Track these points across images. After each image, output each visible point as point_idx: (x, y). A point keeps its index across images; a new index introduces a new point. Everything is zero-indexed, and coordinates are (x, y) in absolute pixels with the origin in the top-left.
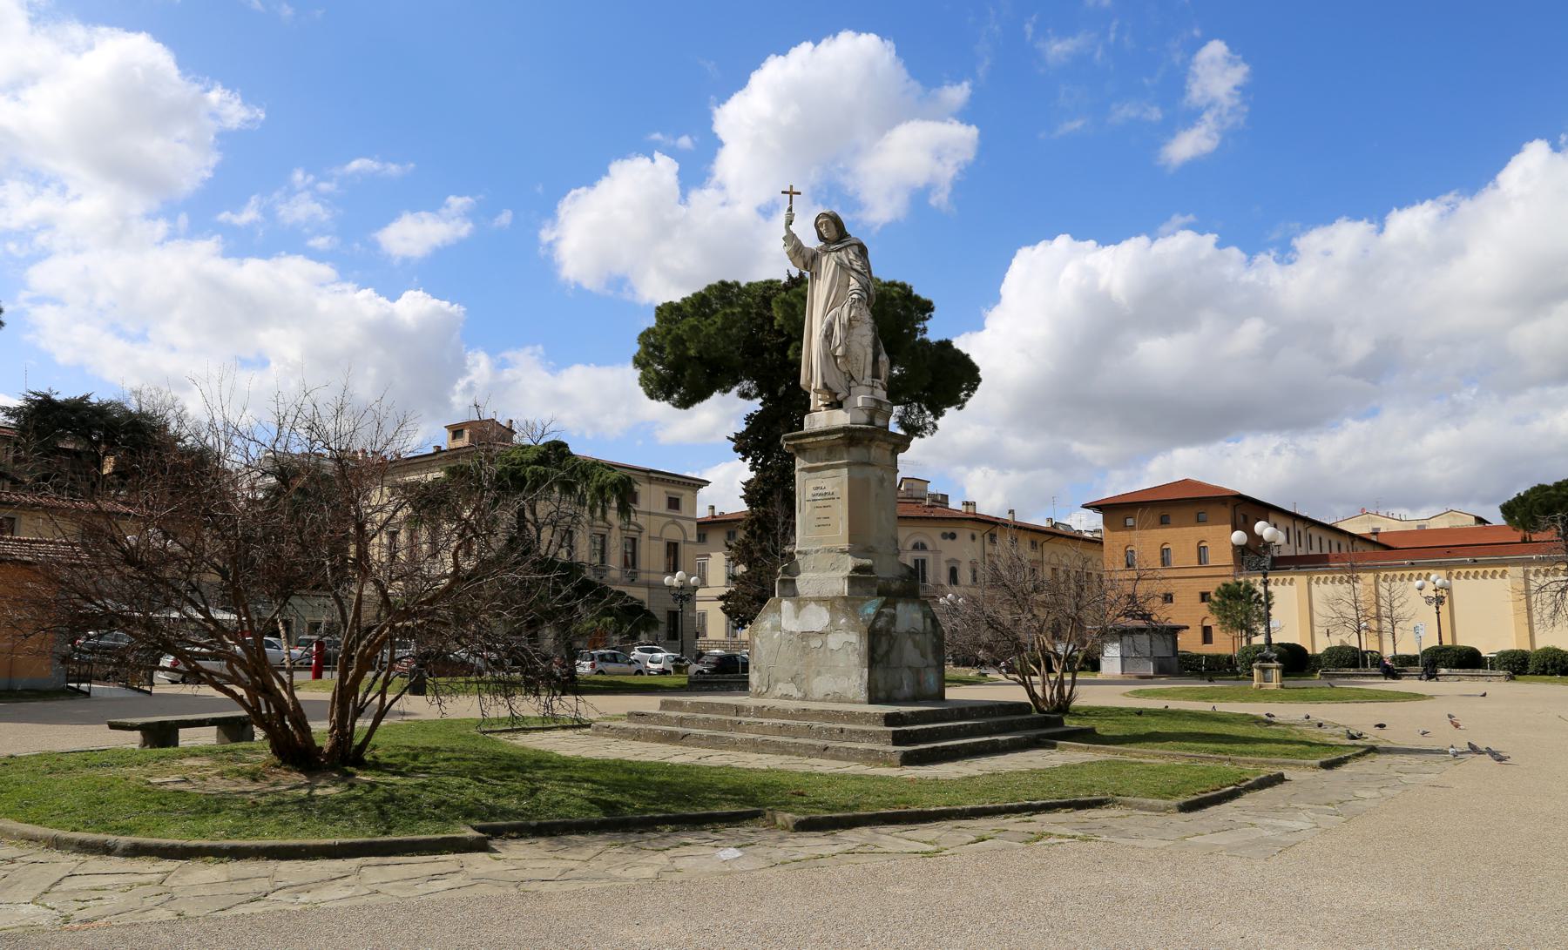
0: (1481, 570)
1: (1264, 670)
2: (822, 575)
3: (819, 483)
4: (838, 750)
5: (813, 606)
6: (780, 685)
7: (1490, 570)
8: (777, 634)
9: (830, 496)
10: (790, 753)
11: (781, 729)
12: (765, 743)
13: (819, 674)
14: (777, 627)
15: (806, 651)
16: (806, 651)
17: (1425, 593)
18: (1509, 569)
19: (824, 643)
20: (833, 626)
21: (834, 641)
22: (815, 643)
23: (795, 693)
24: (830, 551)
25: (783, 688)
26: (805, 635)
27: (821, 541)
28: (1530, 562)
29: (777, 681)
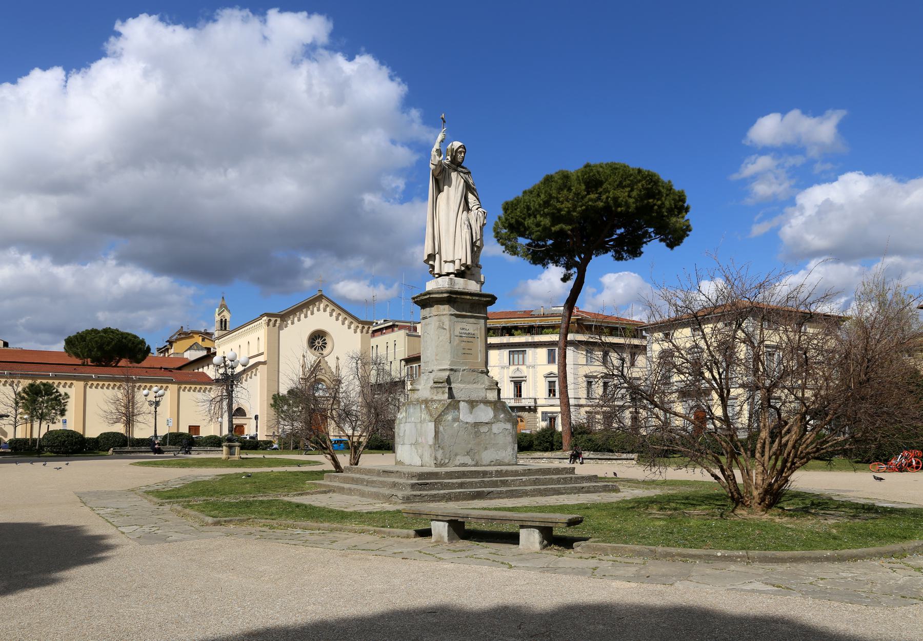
0: (101, 383)
1: (230, 447)
2: (468, 386)
3: (464, 325)
4: (589, 487)
5: (482, 406)
6: (458, 458)
7: (106, 383)
8: (456, 424)
9: (473, 336)
10: (562, 494)
11: (535, 482)
12: (545, 490)
13: (486, 449)
14: (456, 419)
15: (477, 434)
16: (477, 434)
17: (149, 398)
18: (170, 385)
19: (490, 429)
20: (496, 419)
21: (496, 428)
22: (484, 429)
23: (470, 462)
24: (473, 371)
25: (460, 459)
26: (477, 425)
27: (466, 364)
28: (91, 379)
29: (456, 455)
